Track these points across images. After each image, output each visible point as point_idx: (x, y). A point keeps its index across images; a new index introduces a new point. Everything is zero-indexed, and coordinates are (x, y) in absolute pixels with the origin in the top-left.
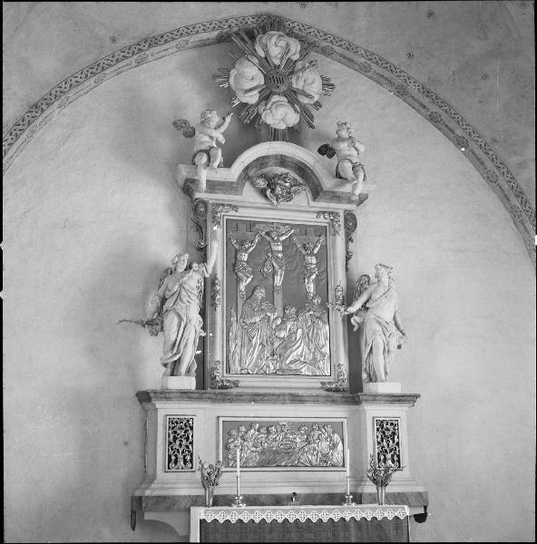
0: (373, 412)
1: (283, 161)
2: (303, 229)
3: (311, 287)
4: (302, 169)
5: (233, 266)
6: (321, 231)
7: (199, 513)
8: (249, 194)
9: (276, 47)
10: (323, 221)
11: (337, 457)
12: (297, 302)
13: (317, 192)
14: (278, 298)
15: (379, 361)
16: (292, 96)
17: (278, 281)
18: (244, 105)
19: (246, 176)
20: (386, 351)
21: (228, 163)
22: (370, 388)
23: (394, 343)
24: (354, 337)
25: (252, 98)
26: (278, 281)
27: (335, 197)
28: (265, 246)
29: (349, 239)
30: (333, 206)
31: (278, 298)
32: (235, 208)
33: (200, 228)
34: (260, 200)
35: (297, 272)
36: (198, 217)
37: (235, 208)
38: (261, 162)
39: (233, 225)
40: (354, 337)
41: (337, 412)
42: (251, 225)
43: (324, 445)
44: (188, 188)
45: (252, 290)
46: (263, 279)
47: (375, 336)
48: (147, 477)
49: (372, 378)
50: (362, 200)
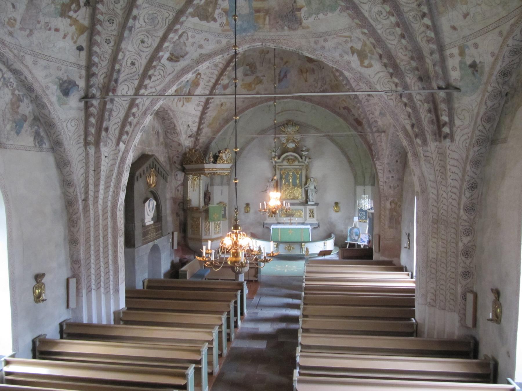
0: (308, 207)
1: (291, 155)
2: (296, 169)
3: (298, 181)
4: (295, 157)
5: (281, 178)
6: (300, 170)
7: (273, 227)
8: (285, 163)
9: (290, 129)
10: (300, 167)
11: (302, 216)
12: (295, 185)
13: (299, 162)
14: (291, 185)
15: (310, 197)
16: (294, 141)
17: (291, 181)
18: (283, 143)
19: (284, 159)
20: (312, 195)
21: (279, 159)
22: (309, 203)
23: (314, 193)
24: (306, 192)
25: (284, 142)
26: (291, 181)
27: (302, 162)
28: (288, 174)
29: (307, 170)
30: (303, 164)
31: (291, 185)
32: (282, 166)
33: (275, 170)
34: (287, 164)
35: (295, 179)
36: (275, 168)
37: (282, 166)
38: (287, 156)
39: (281, 170)
40: (306, 192)
41: (302, 207)
42: (285, 169)
43: (299, 213)
44: (272, 162)
45: (285, 184)
46: (288, 181)
47: (310, 193)
48: (265, 220)
49: (310, 201)
50: (308, 162)
